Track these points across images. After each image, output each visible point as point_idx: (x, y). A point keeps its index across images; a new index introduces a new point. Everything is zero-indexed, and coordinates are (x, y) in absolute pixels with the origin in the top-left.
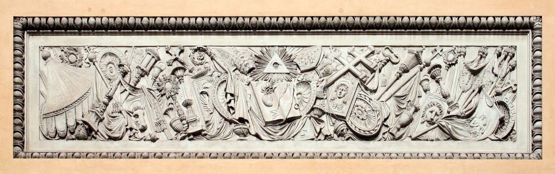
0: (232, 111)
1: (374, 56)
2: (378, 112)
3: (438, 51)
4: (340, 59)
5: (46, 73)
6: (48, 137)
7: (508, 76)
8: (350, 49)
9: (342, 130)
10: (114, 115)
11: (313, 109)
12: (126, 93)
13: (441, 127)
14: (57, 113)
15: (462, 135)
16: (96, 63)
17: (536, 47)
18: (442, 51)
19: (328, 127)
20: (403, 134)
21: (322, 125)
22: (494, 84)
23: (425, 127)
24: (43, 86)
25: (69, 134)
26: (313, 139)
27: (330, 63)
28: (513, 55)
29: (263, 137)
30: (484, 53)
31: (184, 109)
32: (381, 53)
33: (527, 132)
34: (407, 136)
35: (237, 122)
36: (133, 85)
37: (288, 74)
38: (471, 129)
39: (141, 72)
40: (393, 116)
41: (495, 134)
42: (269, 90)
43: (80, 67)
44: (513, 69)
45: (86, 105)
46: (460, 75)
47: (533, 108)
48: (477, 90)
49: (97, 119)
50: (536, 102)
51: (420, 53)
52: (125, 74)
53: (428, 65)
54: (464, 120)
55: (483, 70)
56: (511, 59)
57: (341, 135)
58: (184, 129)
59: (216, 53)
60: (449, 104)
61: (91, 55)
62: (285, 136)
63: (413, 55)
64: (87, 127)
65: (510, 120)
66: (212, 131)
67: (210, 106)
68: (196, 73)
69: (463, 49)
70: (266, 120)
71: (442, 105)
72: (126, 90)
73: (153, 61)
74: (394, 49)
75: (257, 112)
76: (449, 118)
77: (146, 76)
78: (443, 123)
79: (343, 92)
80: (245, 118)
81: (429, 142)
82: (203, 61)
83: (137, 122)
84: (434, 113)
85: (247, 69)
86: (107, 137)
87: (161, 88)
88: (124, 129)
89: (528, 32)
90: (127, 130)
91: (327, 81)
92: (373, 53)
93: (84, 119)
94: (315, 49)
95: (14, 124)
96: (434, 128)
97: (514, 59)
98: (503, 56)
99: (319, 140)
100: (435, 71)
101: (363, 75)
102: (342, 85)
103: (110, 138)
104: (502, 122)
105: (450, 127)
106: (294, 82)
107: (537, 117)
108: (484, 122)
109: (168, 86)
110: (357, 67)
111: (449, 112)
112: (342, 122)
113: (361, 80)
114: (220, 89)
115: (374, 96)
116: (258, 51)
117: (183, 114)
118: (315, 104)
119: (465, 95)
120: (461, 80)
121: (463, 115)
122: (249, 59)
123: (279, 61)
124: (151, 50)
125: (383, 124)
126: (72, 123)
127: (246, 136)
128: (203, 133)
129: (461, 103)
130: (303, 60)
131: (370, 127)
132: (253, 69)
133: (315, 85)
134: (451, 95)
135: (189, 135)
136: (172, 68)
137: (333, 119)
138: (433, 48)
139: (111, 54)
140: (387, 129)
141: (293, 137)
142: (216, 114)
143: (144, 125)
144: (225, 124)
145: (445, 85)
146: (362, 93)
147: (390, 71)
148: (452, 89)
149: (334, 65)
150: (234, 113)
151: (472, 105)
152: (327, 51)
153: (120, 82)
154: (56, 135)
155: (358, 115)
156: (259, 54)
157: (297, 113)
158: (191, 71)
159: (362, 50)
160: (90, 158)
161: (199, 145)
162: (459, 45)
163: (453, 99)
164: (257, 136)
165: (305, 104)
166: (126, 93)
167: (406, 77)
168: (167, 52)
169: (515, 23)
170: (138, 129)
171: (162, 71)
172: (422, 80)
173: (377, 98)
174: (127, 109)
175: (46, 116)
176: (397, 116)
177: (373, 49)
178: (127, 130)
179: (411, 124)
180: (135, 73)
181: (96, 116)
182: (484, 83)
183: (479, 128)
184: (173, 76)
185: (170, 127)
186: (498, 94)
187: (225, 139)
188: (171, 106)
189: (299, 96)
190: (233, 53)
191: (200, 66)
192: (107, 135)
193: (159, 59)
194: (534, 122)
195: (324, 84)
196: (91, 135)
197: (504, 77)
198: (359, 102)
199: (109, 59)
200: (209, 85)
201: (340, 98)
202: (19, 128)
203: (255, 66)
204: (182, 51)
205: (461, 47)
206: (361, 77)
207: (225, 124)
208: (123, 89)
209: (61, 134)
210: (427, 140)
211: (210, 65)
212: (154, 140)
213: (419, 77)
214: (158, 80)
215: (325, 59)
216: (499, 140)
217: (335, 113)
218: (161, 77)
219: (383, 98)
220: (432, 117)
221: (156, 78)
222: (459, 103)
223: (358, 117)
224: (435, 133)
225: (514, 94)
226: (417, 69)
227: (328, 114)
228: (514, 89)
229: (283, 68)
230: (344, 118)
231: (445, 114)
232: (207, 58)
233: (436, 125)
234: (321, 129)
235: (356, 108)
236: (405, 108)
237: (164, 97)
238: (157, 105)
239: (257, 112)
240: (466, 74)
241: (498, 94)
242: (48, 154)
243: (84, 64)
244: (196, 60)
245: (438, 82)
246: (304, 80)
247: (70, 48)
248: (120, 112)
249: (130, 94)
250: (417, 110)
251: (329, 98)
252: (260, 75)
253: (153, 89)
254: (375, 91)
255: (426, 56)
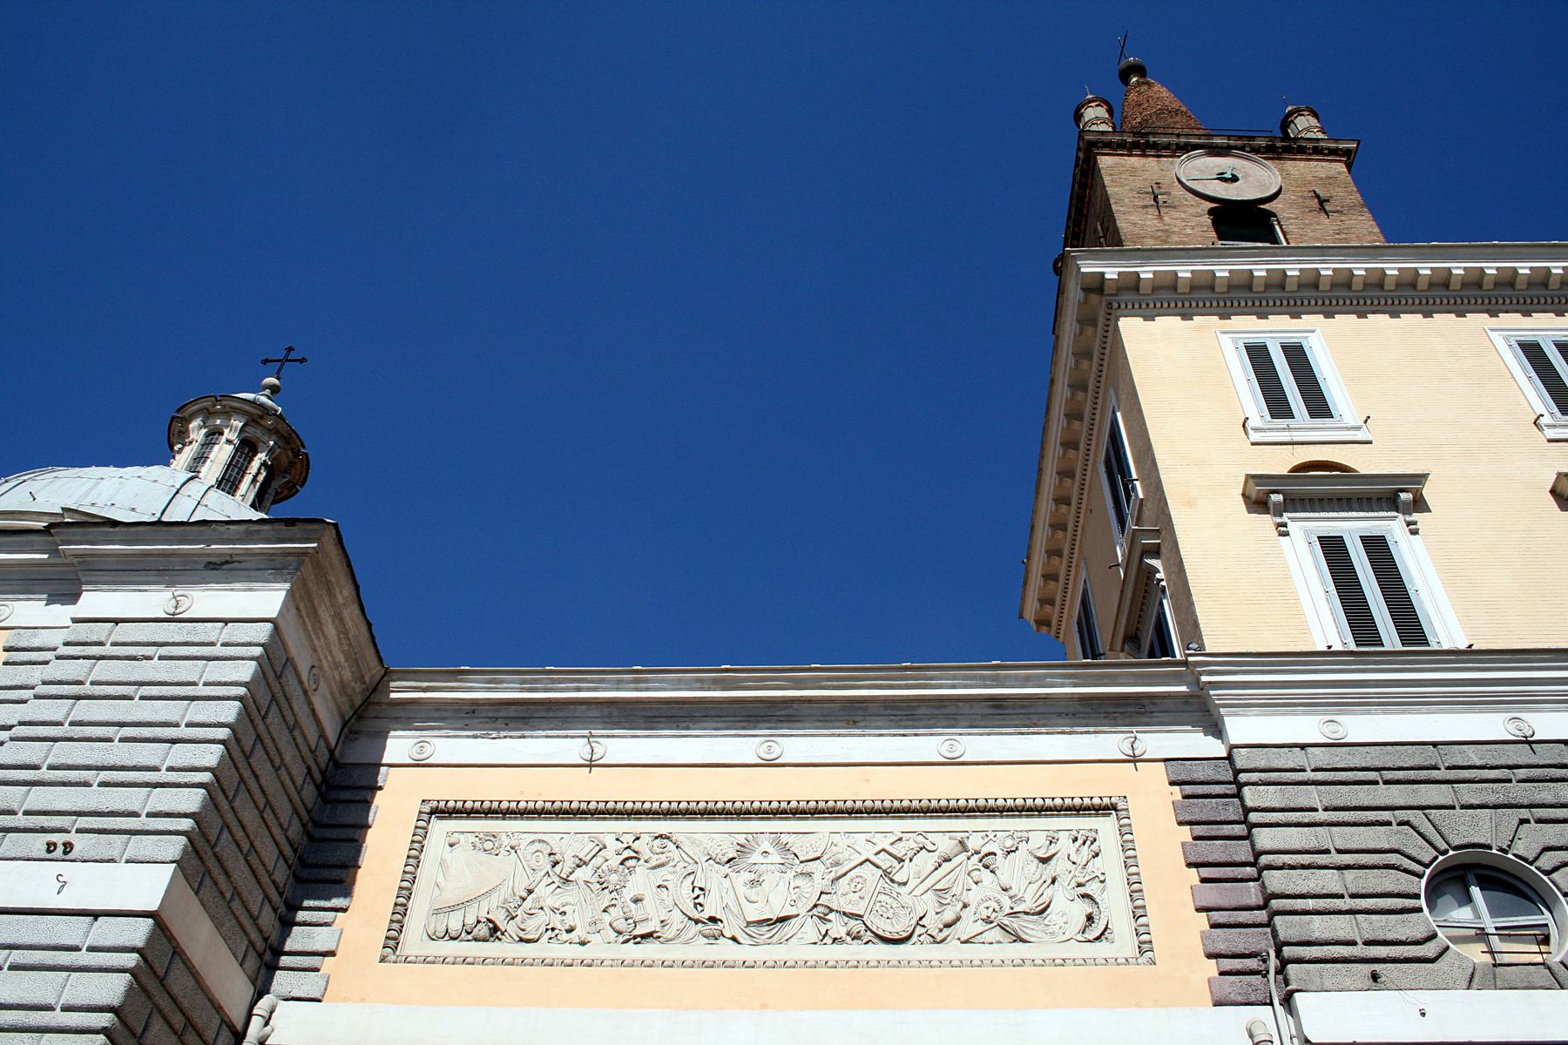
0: (700, 908)
1: (902, 844)
2: (909, 909)
3: (991, 836)
4: (855, 846)
5: (448, 862)
6: (434, 937)
7: (1090, 864)
8: (868, 836)
9: (859, 932)
10: (533, 911)
11: (816, 906)
12: (555, 886)
13: (1002, 927)
14: (452, 909)
15: (1035, 937)
16: (518, 851)
17: (1124, 830)
18: (995, 836)
19: (838, 927)
20: (948, 936)
21: (829, 925)
22: (1072, 873)
23: (980, 926)
24: (442, 877)
25: (464, 934)
26: (815, 943)
27: (841, 851)
28: (1095, 840)
29: (741, 940)
30: (1053, 838)
31: (633, 905)
32: (912, 840)
33: (1127, 929)
34: (953, 938)
35: (707, 921)
36: (565, 876)
37: (783, 864)
38: (1046, 928)
39: (578, 862)
40: (931, 913)
41: (1083, 933)
42: (754, 883)
43: (497, 855)
44: (1097, 855)
45: (495, 900)
46: (1023, 863)
47: (1132, 900)
48: (1049, 881)
49: (507, 916)
50: (1135, 893)
51: (966, 840)
52: (556, 864)
53: (977, 852)
54: (1035, 917)
55: (1056, 857)
56: (1092, 843)
57: (857, 937)
58: (629, 930)
59: (684, 840)
60: (1011, 898)
61: (514, 842)
62: (774, 940)
63: (957, 842)
64: (491, 925)
65: (1102, 916)
66: (669, 933)
67: (669, 903)
68: (653, 863)
69: (1025, 834)
70: (748, 920)
71: (1002, 899)
72: (553, 882)
73: (597, 849)
74: (928, 835)
75: (735, 910)
76: (1013, 914)
77: (584, 866)
78: (1006, 922)
79: (859, 886)
80: (718, 917)
81: (987, 945)
82: (665, 849)
83: (563, 920)
84: (991, 909)
85: (726, 859)
86: (517, 939)
87: (602, 880)
88: (543, 928)
89: (1111, 814)
90: (547, 930)
91: (836, 872)
92: (900, 839)
93: (489, 916)
94: (821, 836)
95: (391, 920)
96: (993, 928)
97: (1096, 844)
98: (1080, 841)
99: (825, 944)
100: (986, 860)
101: (888, 865)
102: (857, 877)
103: (521, 940)
104: (1090, 918)
105: (1015, 926)
106: (790, 874)
107: (1139, 912)
108: (1065, 919)
109: (614, 878)
110: (878, 856)
111: (1012, 908)
112: (858, 922)
113: (884, 871)
114: (684, 883)
115: (902, 890)
116: (741, 839)
117: (630, 911)
118: (819, 899)
119: (1034, 887)
120: (1025, 868)
121: (1033, 911)
122: (729, 847)
123: (770, 849)
124: (595, 838)
125: (918, 924)
126: (471, 920)
127: (717, 939)
128: (655, 935)
129: (1028, 897)
130: (804, 848)
131: (898, 928)
132: (734, 858)
133: (820, 878)
134: (1014, 888)
135: (635, 937)
136: (621, 858)
137: (844, 917)
138: (984, 833)
139: (540, 841)
140: (924, 930)
141: (787, 940)
142: (676, 912)
143: (573, 924)
144: (688, 924)
145: (1004, 876)
146: (886, 885)
147: (926, 861)
148: (1014, 882)
149: (846, 854)
150: (703, 910)
151: (1045, 898)
152: (836, 838)
153: (548, 872)
154: (445, 935)
155: (880, 913)
156: (743, 841)
157: (793, 911)
158: (646, 861)
159: (886, 837)
160: (487, 964)
161: (649, 950)
162: (1019, 829)
163: (1017, 892)
164: (734, 939)
165: (804, 900)
166: (555, 886)
167: (946, 867)
168: (617, 839)
169: (1092, 804)
170: (563, 929)
171: (607, 860)
172: (970, 869)
173: (908, 892)
174: (551, 905)
175: (437, 912)
176: (937, 913)
177: (900, 835)
178: (547, 930)
179: (958, 924)
180: (569, 863)
181: (507, 914)
182: (1059, 873)
183: (1057, 926)
184: (621, 866)
185: (609, 927)
186: (1080, 885)
187: (687, 943)
188: (614, 902)
189: (796, 890)
190: (706, 841)
191: (660, 855)
192: (518, 936)
193: (605, 847)
194: (1136, 918)
195: (832, 876)
196: (495, 935)
197: (1086, 865)
198: (882, 897)
199: (537, 846)
200: (669, 877)
201: (854, 892)
202: (396, 926)
203: (736, 856)
204: (638, 838)
205: (1021, 831)
206: (884, 868)
207: (688, 924)
208: (550, 881)
209: (454, 934)
210: (983, 943)
211: (675, 853)
212: (583, 943)
213: (967, 866)
214: (600, 870)
215: (833, 847)
216: (1090, 941)
217: (847, 911)
218: (604, 867)
219: (917, 892)
220: (989, 915)
221: (598, 868)
222: (1025, 896)
223: (882, 915)
224: (996, 934)
225: (1103, 885)
226: (963, 856)
227: (837, 911)
228: (1102, 878)
229: (776, 857)
230: (862, 916)
231: (1008, 911)
232: (671, 846)
233: (995, 924)
234: (827, 931)
235: (878, 904)
236: (949, 904)
237: (606, 891)
238: (594, 900)
239: (735, 910)
240: (1032, 862)
241: (1080, 885)
242: (428, 959)
243: (503, 852)
244: (656, 849)
245: (992, 872)
246: (804, 871)
247: (487, 834)
248: (542, 908)
249: (558, 887)
250: (965, 906)
251: (839, 893)
252: (742, 866)
253: (592, 881)
254: (905, 884)
255: (974, 843)
